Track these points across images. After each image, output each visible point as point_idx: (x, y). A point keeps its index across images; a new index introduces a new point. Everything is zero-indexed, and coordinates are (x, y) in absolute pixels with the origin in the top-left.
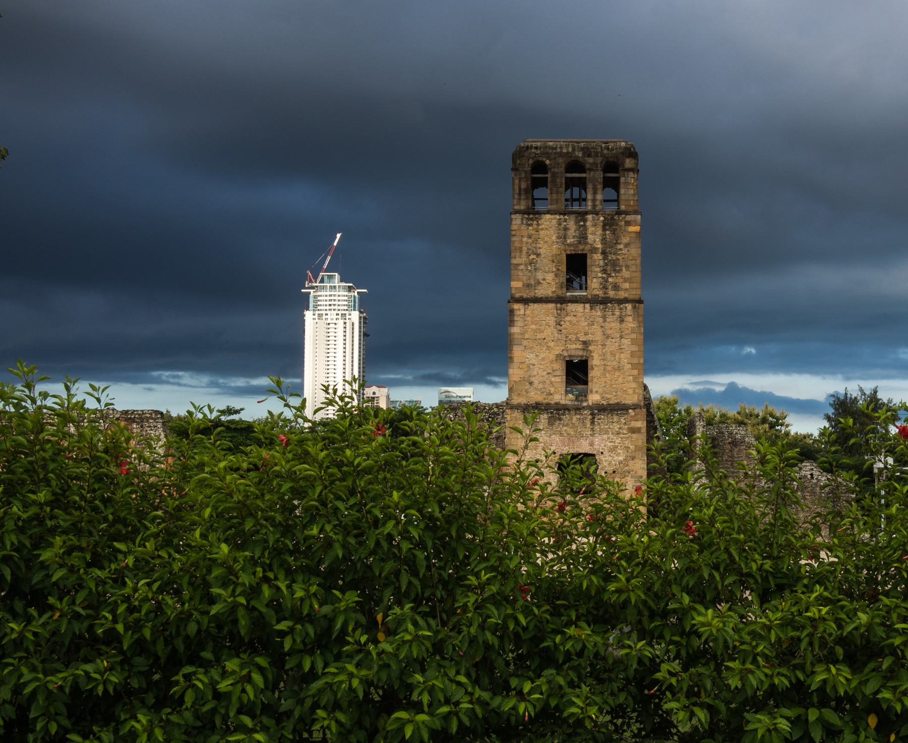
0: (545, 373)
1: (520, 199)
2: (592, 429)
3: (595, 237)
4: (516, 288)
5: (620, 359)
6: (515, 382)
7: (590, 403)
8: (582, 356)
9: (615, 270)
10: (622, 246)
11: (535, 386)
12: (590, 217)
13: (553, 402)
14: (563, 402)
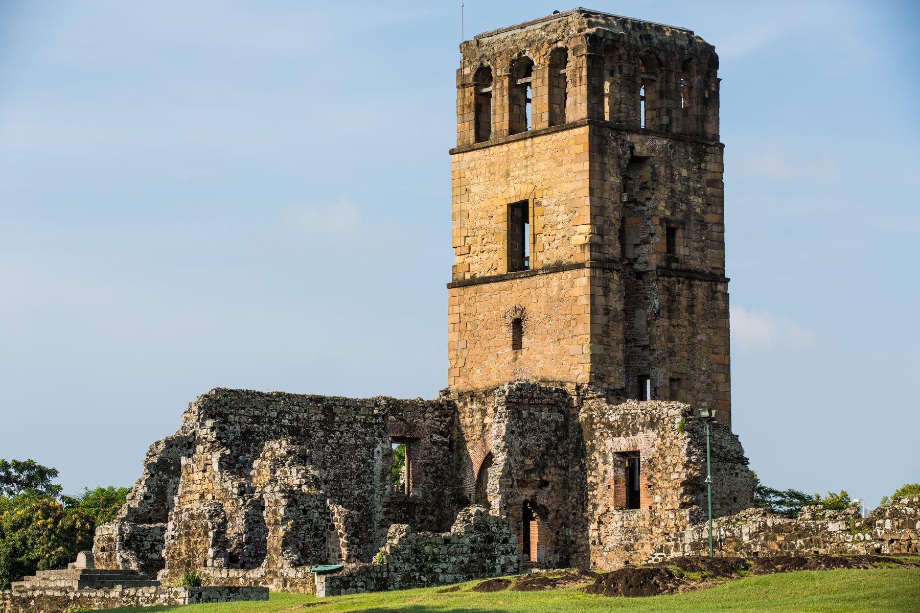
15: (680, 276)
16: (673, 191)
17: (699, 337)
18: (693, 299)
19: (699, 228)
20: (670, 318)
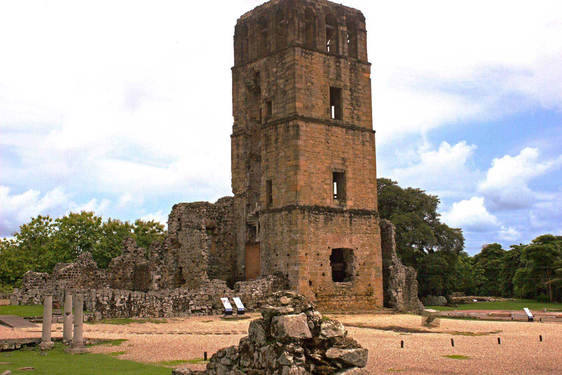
0: (320, 181)
1: (299, 36)
2: (351, 230)
3: (346, 76)
4: (299, 108)
5: (364, 175)
6: (301, 186)
7: (348, 209)
8: (342, 170)
9: (357, 105)
10: (360, 87)
11: (315, 190)
12: (342, 60)
13: (325, 206)
14: (332, 206)
15: (270, 126)
16: (269, 82)
17: (280, 155)
18: (277, 135)
19: (282, 95)
20: (266, 149)
